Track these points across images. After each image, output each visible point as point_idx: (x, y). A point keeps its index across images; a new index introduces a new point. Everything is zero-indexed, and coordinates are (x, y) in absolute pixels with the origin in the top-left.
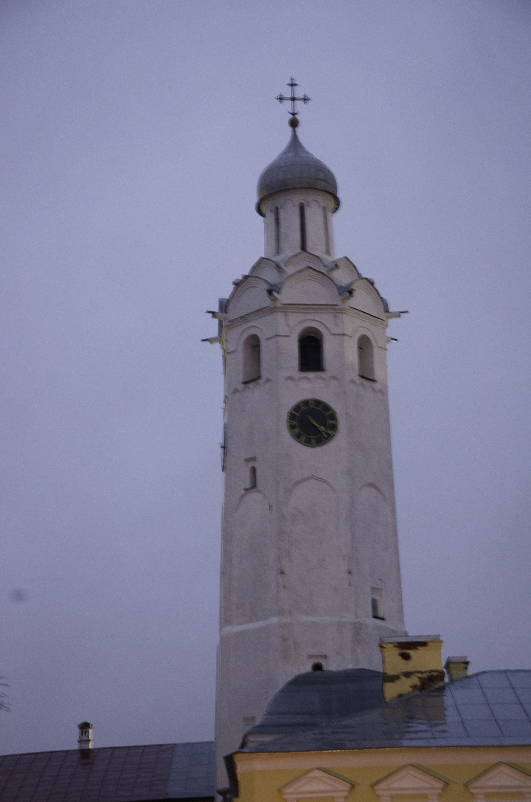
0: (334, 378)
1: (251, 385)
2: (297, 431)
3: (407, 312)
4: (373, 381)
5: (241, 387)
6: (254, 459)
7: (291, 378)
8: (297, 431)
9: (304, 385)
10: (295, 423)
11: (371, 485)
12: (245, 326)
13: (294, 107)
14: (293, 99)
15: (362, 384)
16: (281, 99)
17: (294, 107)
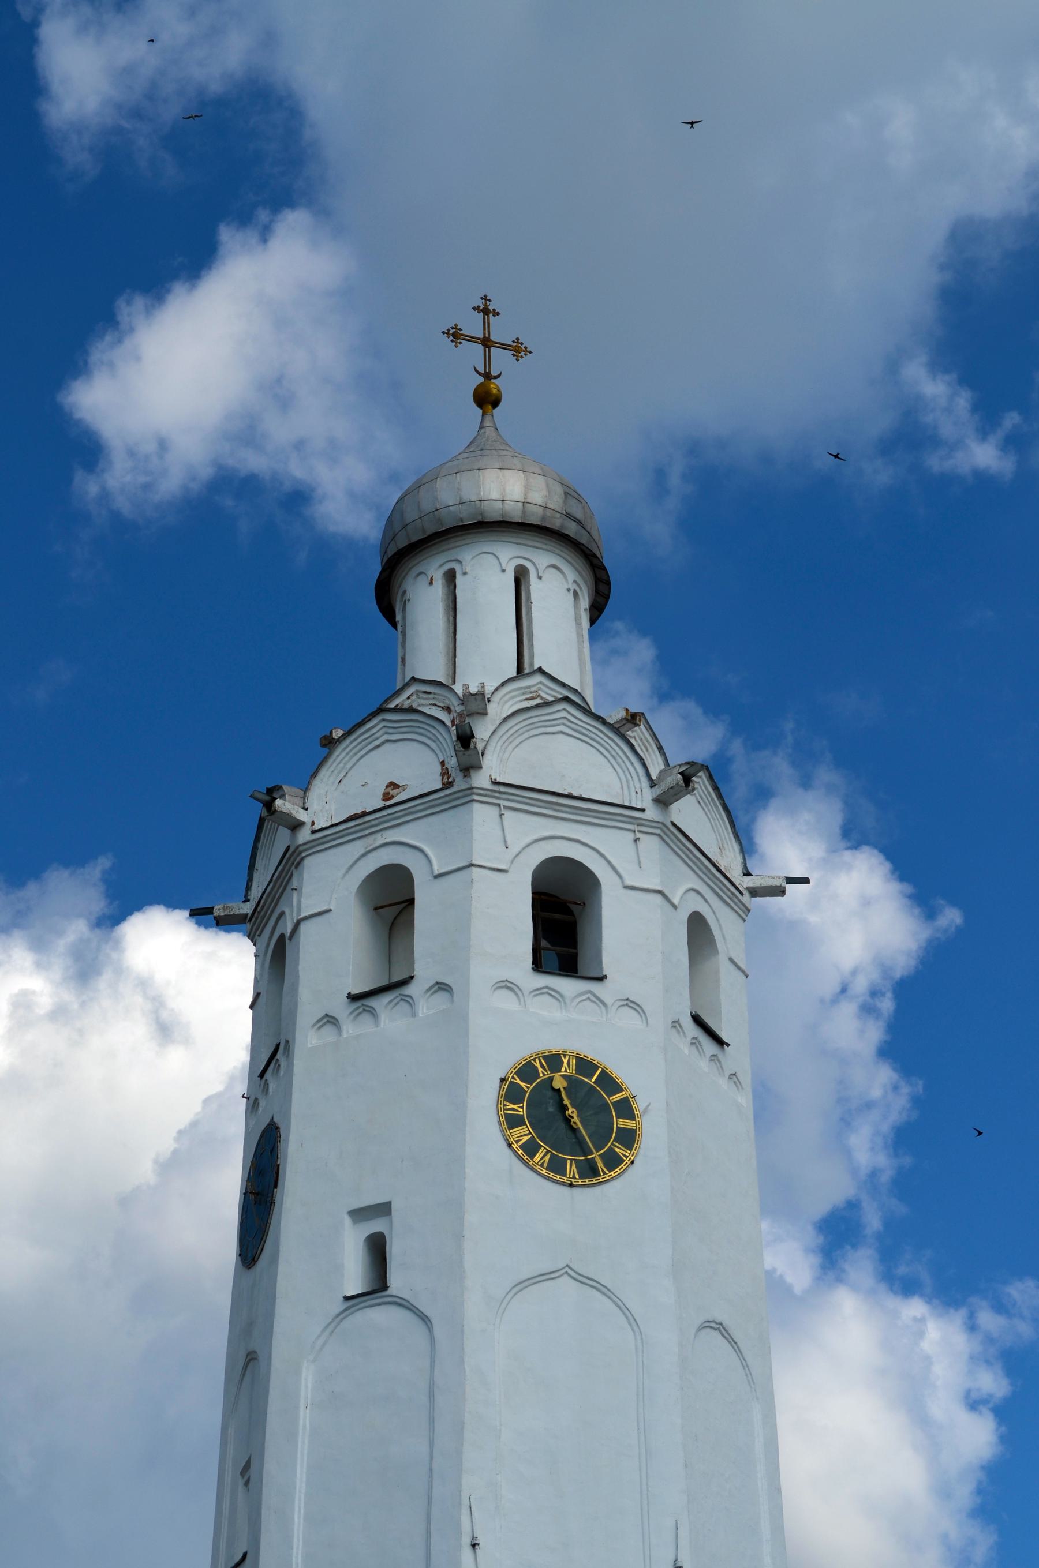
0: (629, 1003)
1: (379, 1003)
2: (522, 1134)
3: (805, 881)
4: (720, 1042)
5: (340, 1008)
6: (383, 1209)
7: (507, 986)
8: (522, 1134)
9: (544, 1009)
10: (520, 1110)
11: (719, 1327)
12: (357, 848)
13: (487, 360)
14: (486, 343)
15: (695, 1042)
16: (456, 335)
17: (487, 360)
